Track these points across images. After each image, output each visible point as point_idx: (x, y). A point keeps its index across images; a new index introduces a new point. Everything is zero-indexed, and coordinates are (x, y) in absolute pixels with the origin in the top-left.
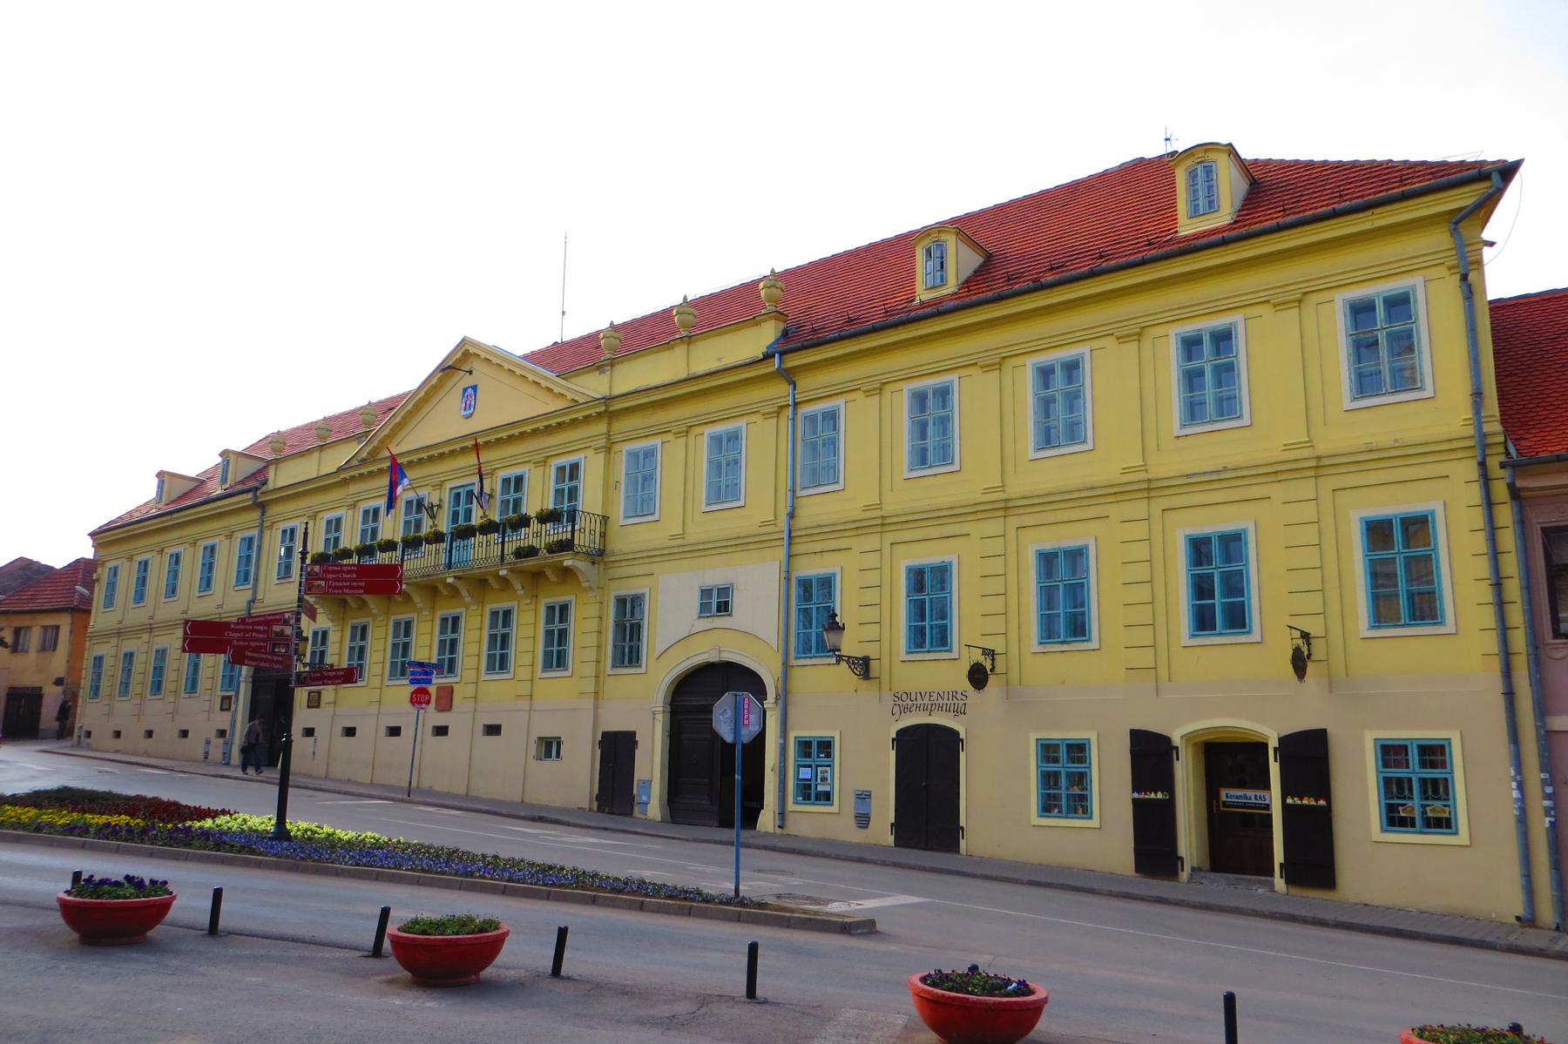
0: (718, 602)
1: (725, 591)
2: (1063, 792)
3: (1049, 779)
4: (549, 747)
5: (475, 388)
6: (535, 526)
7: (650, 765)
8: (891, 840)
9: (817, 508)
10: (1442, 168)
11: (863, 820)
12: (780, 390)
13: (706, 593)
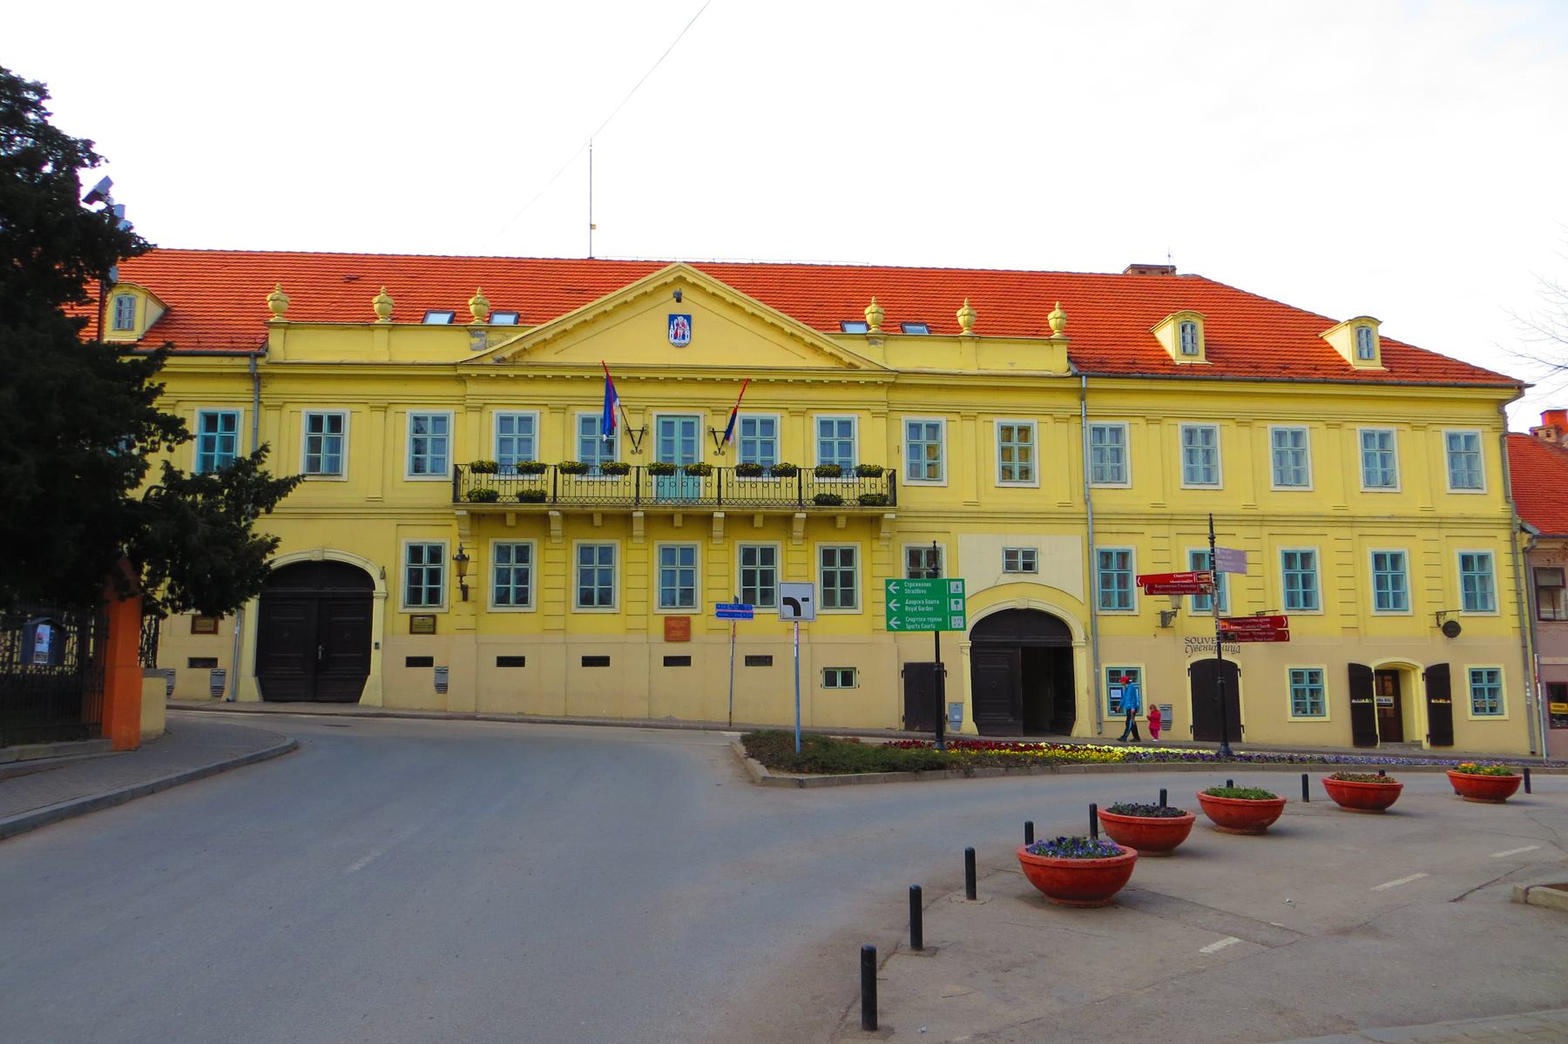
0: (1022, 562)
1: (1029, 554)
3: (1297, 693)
5: (688, 318)
7: (959, 688)
9: (1108, 498)
10: (1488, 374)
12: (1072, 402)
13: (1010, 555)
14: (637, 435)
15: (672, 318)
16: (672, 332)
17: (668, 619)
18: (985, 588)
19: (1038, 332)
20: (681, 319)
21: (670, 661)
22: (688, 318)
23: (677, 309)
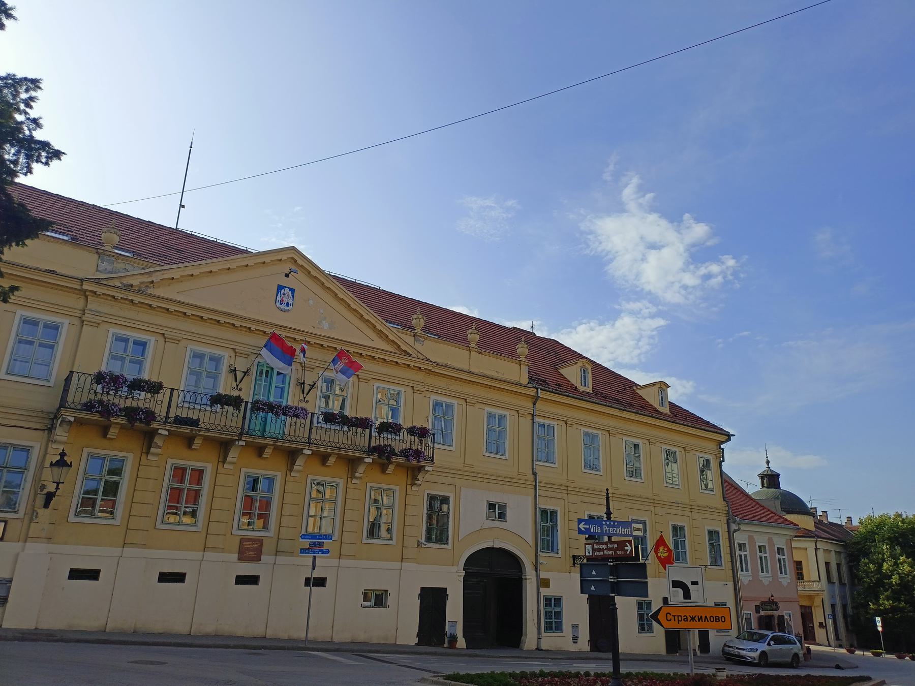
0: (497, 511)
1: (503, 507)
2: (554, 620)
4: (379, 599)
6: (404, 435)
7: (455, 611)
8: (588, 649)
11: (575, 639)
13: (492, 506)
14: (239, 375)
15: (280, 288)
16: (279, 299)
17: (242, 540)
18: (471, 530)
19: (513, 355)
20: (287, 290)
21: (242, 580)
22: (293, 290)
23: (284, 281)
